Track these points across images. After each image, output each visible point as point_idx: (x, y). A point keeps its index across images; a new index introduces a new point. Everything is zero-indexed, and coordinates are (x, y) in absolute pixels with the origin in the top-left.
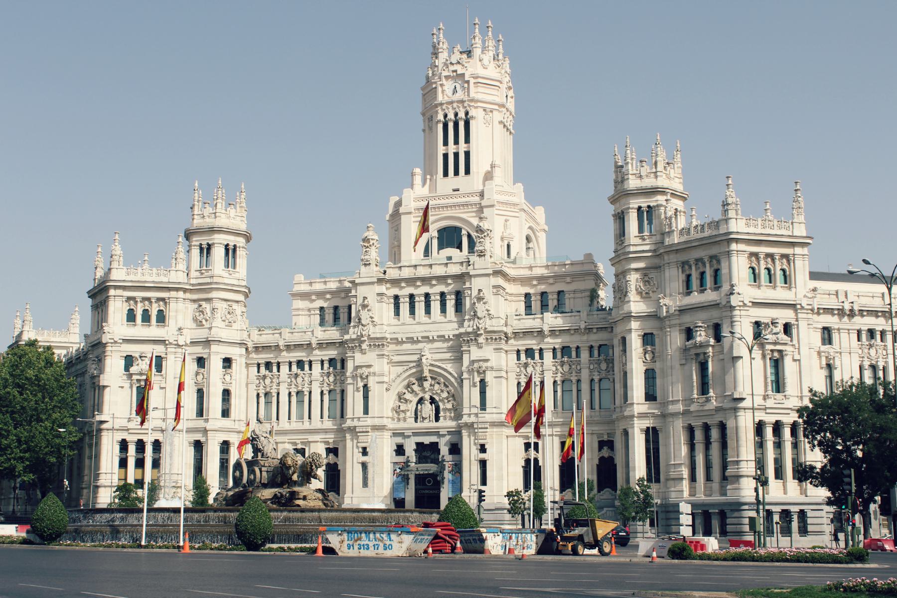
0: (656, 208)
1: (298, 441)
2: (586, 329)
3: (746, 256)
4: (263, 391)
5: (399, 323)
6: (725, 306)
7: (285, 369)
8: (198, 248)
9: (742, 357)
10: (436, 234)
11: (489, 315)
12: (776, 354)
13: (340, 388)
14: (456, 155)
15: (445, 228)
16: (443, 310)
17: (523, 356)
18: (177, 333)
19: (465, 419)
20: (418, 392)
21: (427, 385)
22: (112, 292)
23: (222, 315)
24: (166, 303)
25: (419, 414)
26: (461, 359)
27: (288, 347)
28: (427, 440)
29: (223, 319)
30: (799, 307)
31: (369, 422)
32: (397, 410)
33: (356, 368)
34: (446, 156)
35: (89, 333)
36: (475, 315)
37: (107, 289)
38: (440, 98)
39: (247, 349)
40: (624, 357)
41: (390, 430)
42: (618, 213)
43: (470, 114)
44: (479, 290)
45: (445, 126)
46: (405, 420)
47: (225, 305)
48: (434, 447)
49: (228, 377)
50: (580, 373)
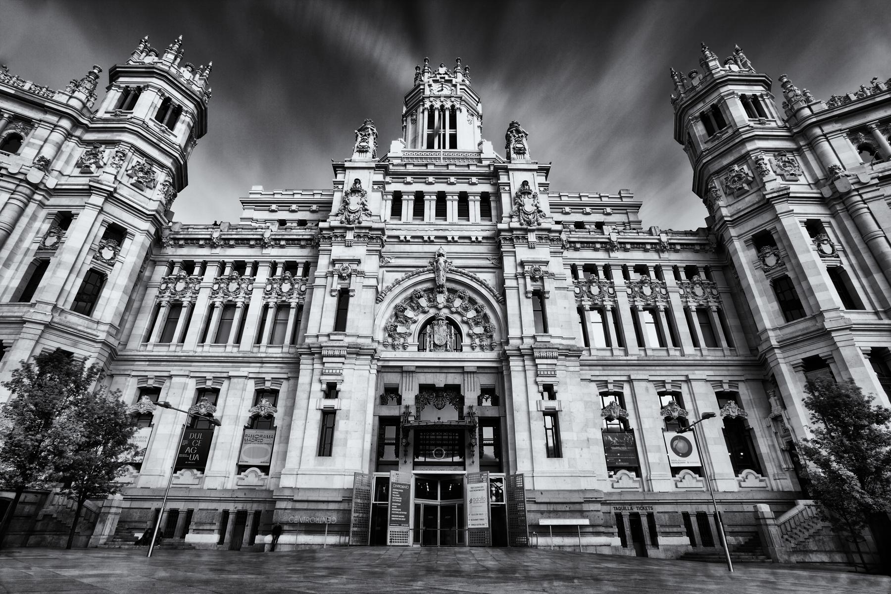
1: (209, 376)
4: (168, 299)
11: (540, 211)
13: (297, 300)
17: (581, 274)
20: (427, 309)
21: (441, 299)
25: (428, 339)
28: (440, 380)
29: (130, 172)
31: (348, 340)
32: (391, 331)
33: (333, 263)
38: (427, 92)
40: (771, 261)
41: (378, 360)
44: (525, 183)
46: (404, 348)
47: (136, 159)
48: (454, 393)
49: (107, 254)
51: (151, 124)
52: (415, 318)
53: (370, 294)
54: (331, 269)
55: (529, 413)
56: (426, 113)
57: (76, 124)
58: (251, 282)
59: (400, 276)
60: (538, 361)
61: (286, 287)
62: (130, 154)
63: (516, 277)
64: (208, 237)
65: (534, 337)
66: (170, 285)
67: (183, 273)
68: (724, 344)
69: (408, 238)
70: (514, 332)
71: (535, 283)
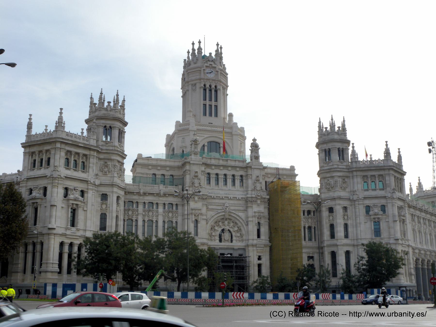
5: (211, 188)
6: (389, 198)
7: (141, 207)
10: (206, 144)
11: (262, 189)
14: (210, 106)
15: (211, 142)
18: (94, 177)
19: (251, 242)
20: (222, 226)
21: (226, 222)
22: (58, 145)
24: (87, 158)
26: (246, 210)
27: (145, 194)
32: (211, 235)
34: (205, 105)
35: (21, 170)
36: (255, 189)
37: (55, 142)
40: (331, 218)
42: (325, 149)
43: (218, 87)
45: (205, 90)
46: (215, 240)
49: (118, 208)
51: (119, 147)
54: (191, 212)
55: (254, 264)
56: (202, 90)
58: (157, 212)
60: (258, 248)
61: (170, 215)
63: (252, 217)
65: (257, 240)
66: (126, 212)
68: (313, 240)
69: (215, 197)
70: (251, 237)
71: (258, 220)
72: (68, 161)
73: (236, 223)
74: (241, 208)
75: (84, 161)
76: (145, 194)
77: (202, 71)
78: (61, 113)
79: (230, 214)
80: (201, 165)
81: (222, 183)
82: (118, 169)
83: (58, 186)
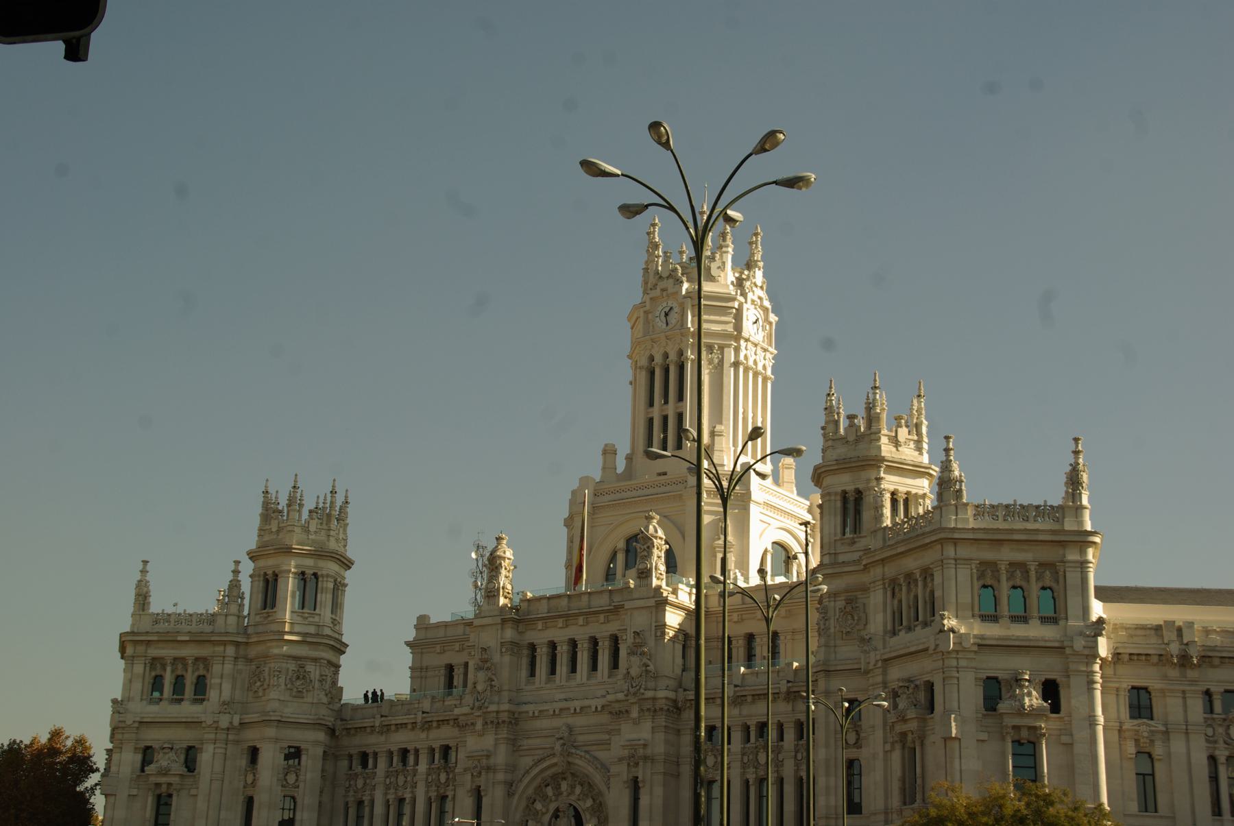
0: (867, 493)
2: (788, 693)
3: (973, 566)
4: (352, 799)
8: (262, 579)
9: (960, 739)
10: (621, 545)
12: (1024, 734)
14: (665, 418)
16: (594, 667)
21: (564, 786)
23: (288, 681)
26: (608, 743)
29: (289, 686)
30: (1068, 651)
34: (650, 421)
39: (332, 732)
44: (634, 632)
45: (652, 373)
47: (292, 666)
49: (291, 778)
50: (782, 765)
52: (544, 810)
53: (499, 792)
57: (237, 644)
58: (415, 772)
59: (526, 761)
62: (284, 665)
64: (372, 724)
66: (352, 782)
67: (359, 769)
71: (633, 769)
72: (157, 684)
73: (589, 783)
74: (607, 737)
75: (202, 672)
76: (386, 729)
77: (642, 314)
78: (144, 572)
79: (570, 759)
80: (499, 626)
81: (565, 669)
82: (288, 677)
83: (121, 748)
